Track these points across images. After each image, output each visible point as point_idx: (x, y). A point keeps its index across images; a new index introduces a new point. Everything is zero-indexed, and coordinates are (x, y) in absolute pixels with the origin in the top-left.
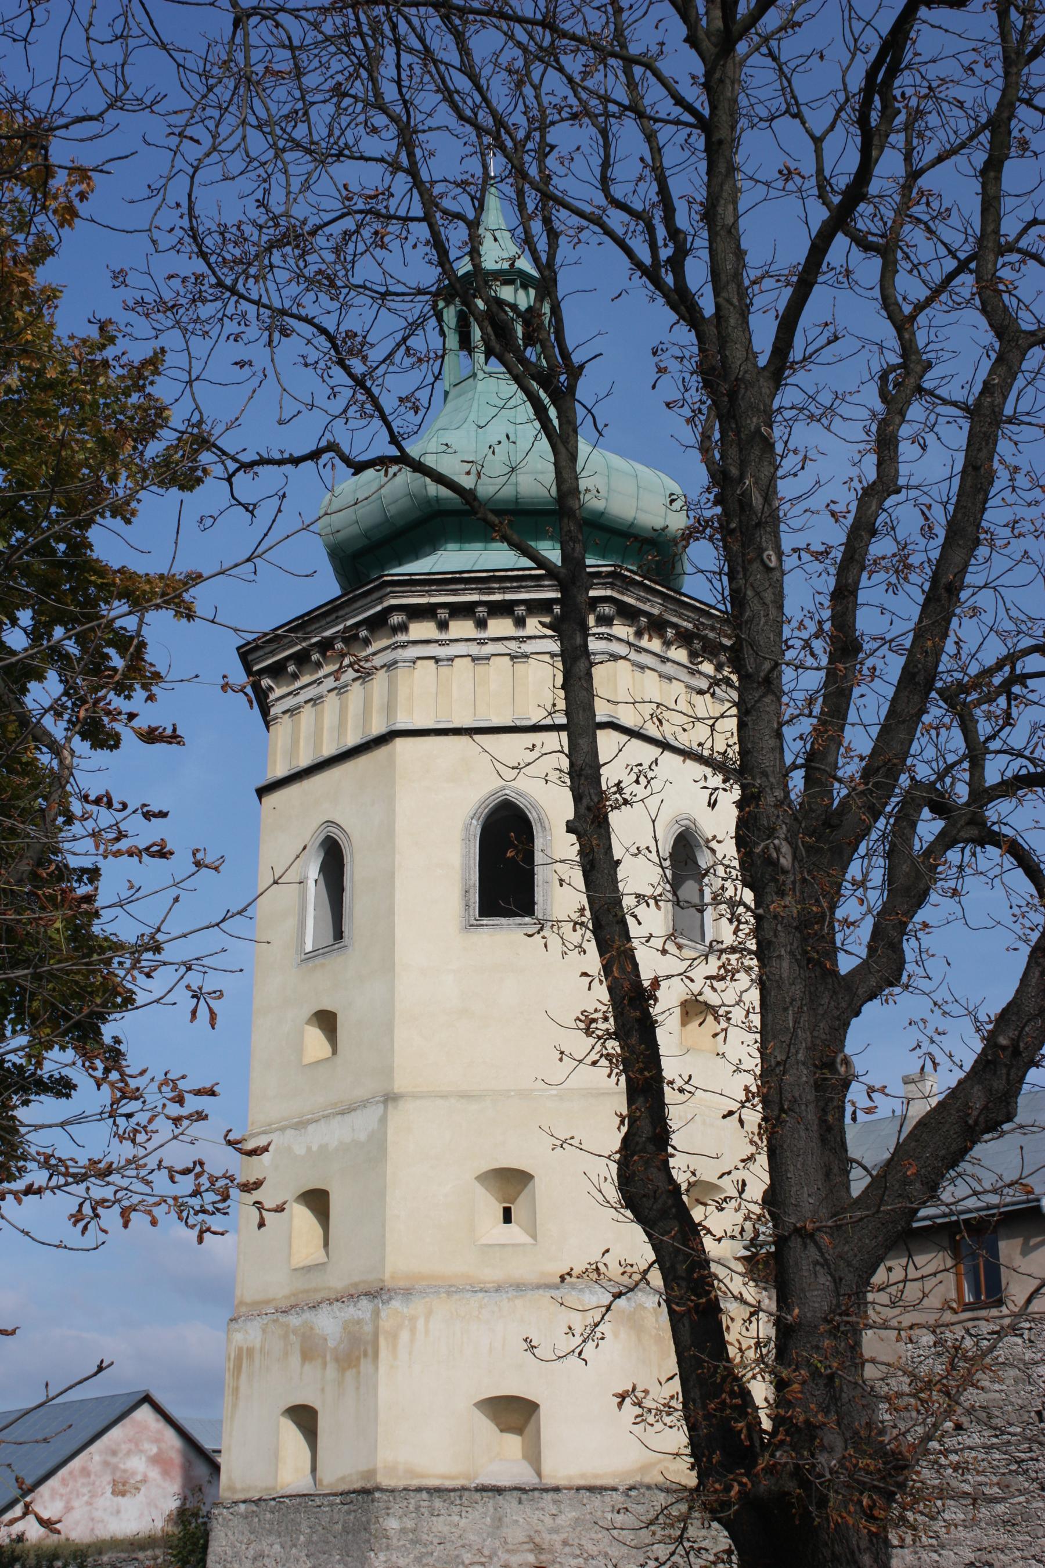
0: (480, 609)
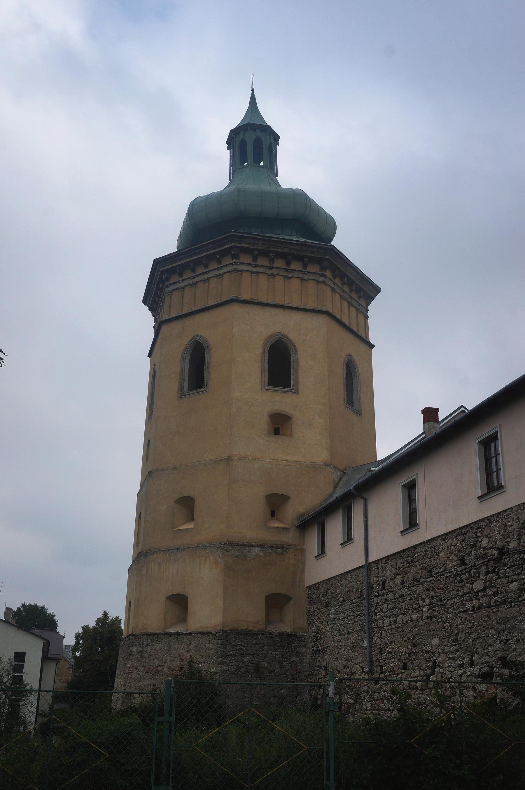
0: (191, 264)
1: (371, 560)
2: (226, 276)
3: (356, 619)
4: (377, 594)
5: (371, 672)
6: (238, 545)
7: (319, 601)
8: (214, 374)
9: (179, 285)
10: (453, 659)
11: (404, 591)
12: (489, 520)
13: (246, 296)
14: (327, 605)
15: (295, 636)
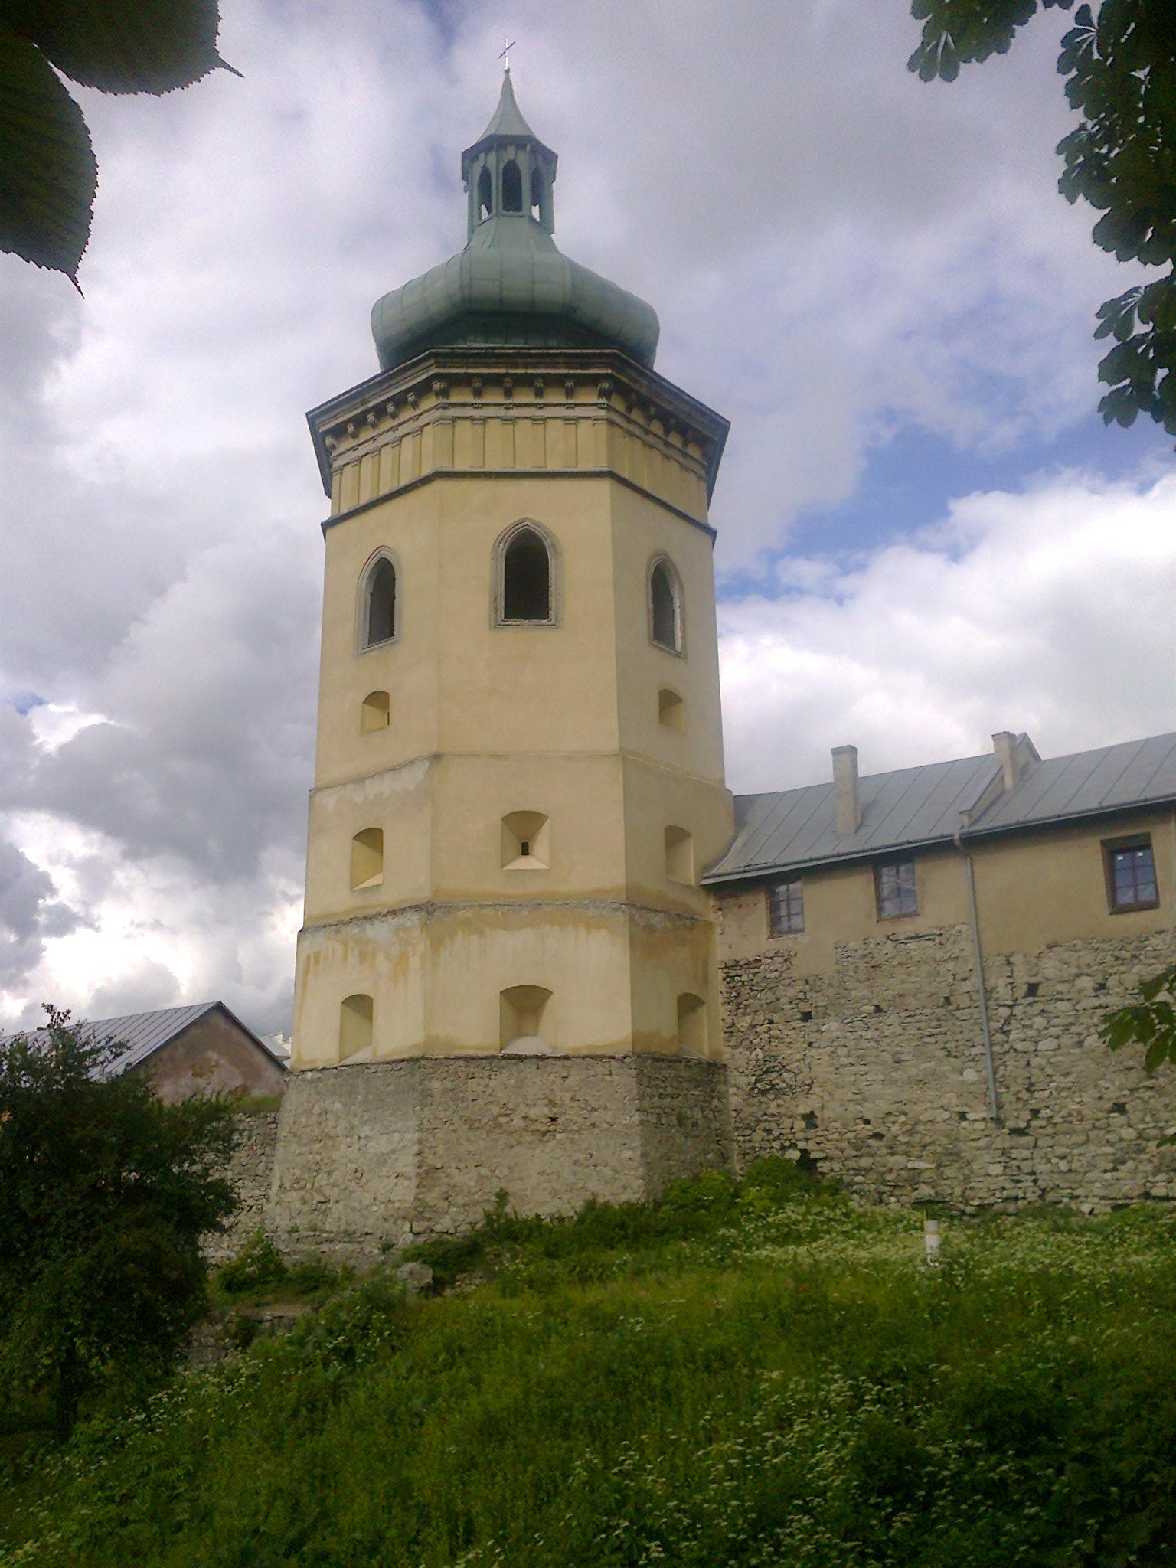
2: (584, 425)
3: (932, 1040)
4: (1010, 1003)
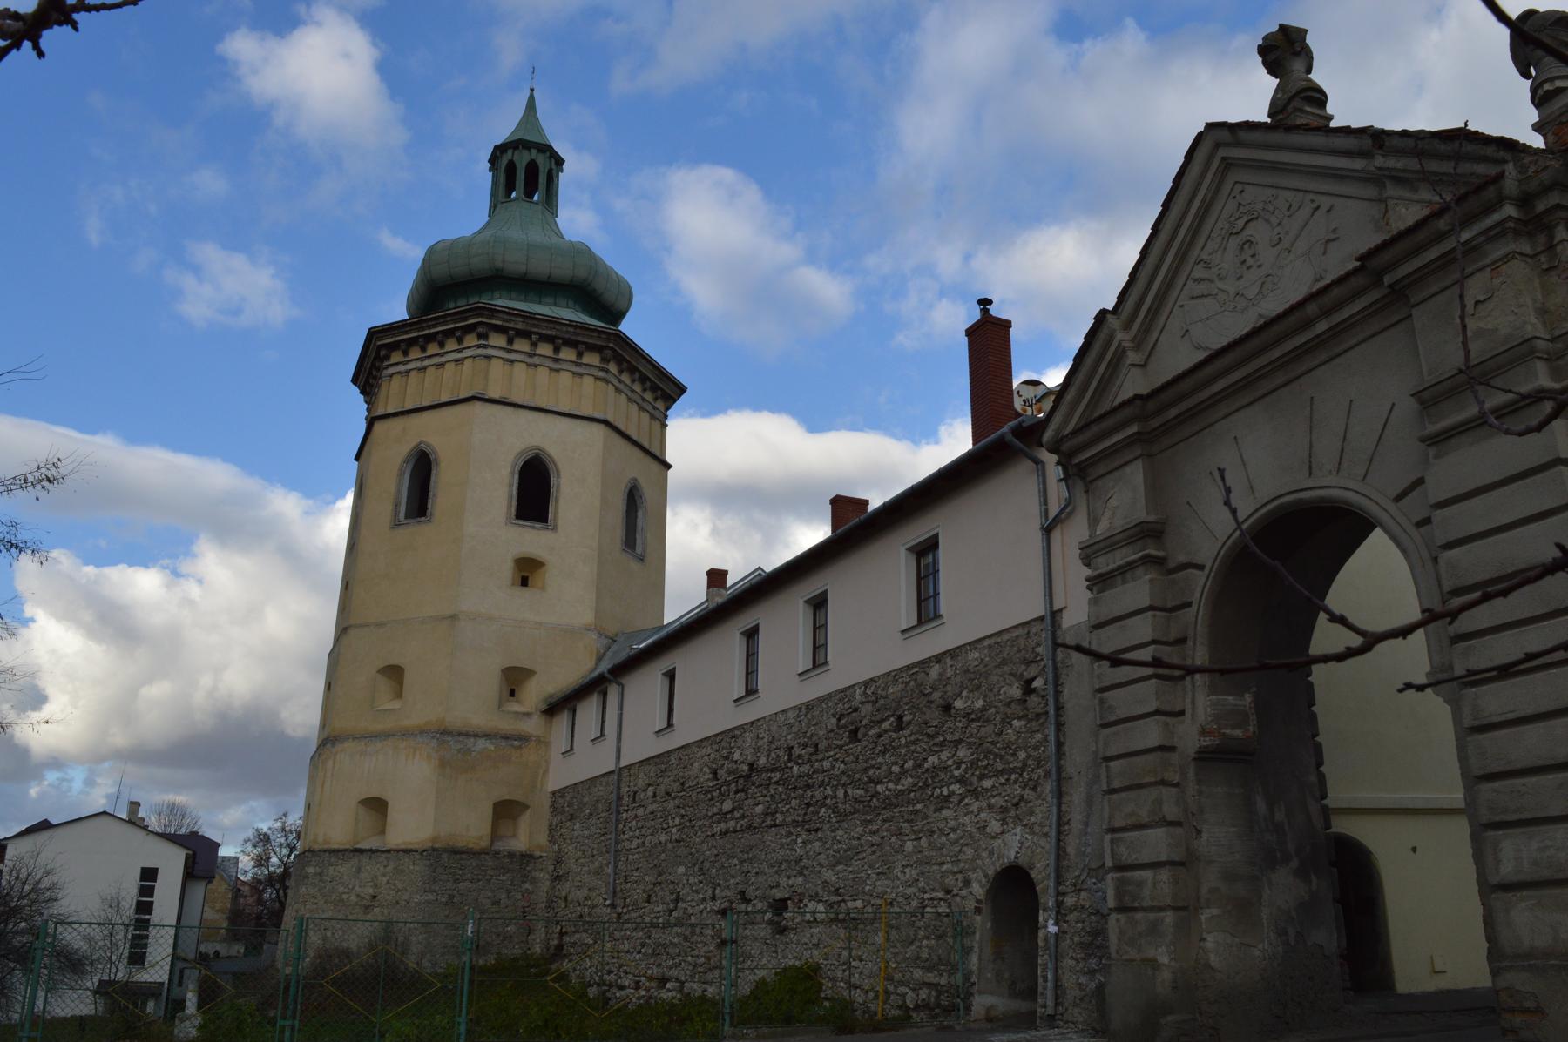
1: (623, 764)
2: (468, 363)
5: (613, 906)
6: (460, 734)
7: (563, 812)
8: (441, 499)
9: (402, 368)
10: (697, 892)
11: (655, 806)
12: (742, 728)
13: (494, 393)
14: (572, 818)
15: (531, 856)
